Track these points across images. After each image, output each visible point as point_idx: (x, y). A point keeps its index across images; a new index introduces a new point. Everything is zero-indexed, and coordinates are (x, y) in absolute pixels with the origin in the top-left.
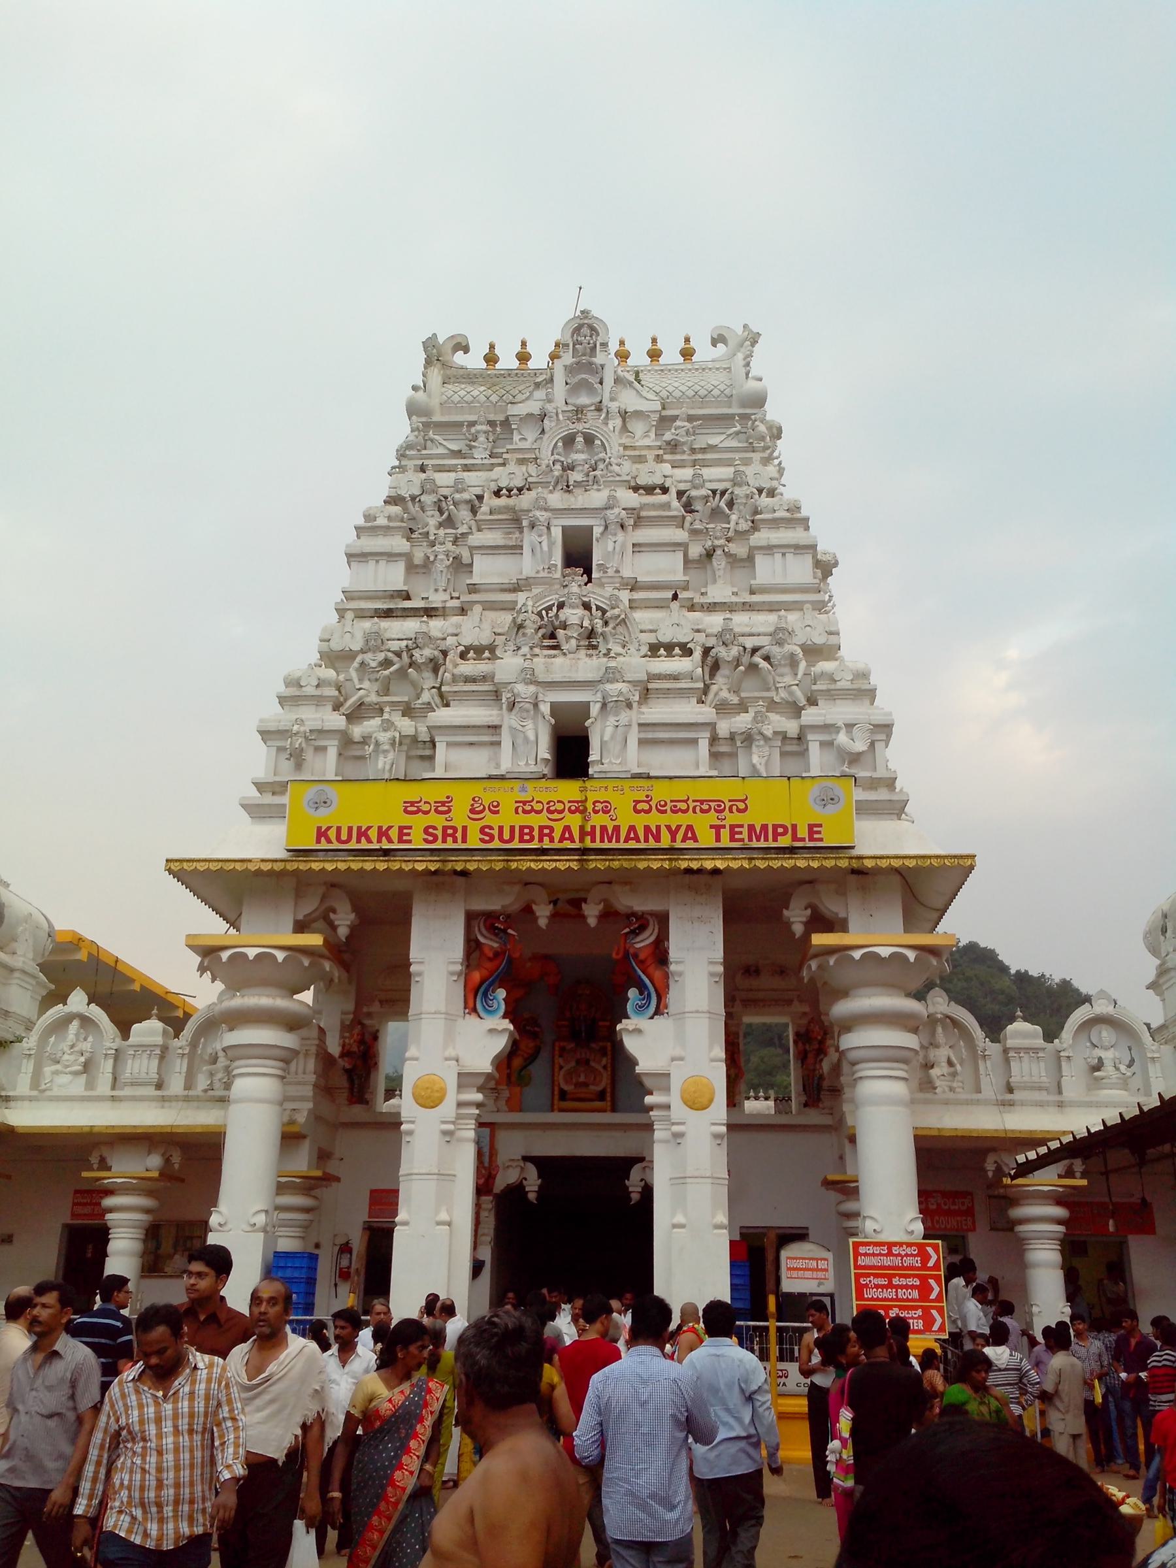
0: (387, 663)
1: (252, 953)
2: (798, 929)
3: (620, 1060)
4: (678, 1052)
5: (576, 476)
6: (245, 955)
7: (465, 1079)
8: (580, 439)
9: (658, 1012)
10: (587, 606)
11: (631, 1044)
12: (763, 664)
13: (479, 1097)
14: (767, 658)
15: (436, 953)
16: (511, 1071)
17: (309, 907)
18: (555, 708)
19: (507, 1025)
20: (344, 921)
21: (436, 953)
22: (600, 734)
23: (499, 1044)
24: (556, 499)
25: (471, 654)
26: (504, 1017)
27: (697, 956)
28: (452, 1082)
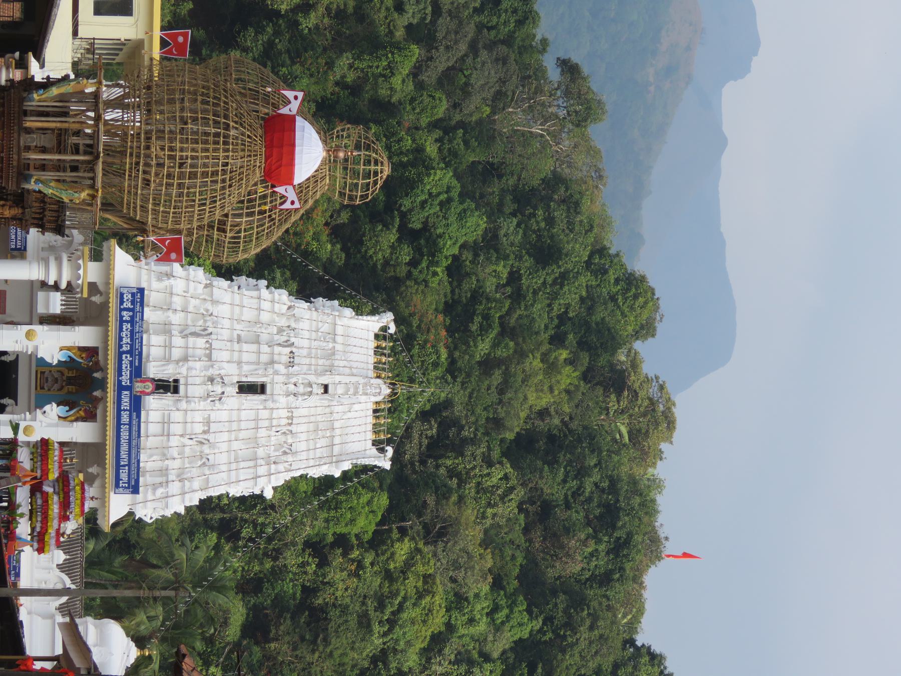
0: (207, 311)
1: (81, 272)
2: (90, 470)
3: (40, 405)
4: (44, 424)
5: (292, 387)
6: (79, 269)
7: (36, 348)
8: (309, 389)
9: (59, 417)
10: (223, 393)
11: (47, 408)
12: (200, 463)
13: (29, 353)
14: (204, 463)
15: (83, 336)
16: (41, 362)
17: (101, 287)
18: (176, 381)
19: (55, 362)
20: (96, 299)
21: (83, 336)
22: (168, 399)
23: (49, 360)
24: (280, 379)
25: (208, 346)
26: (59, 361)
27: (81, 432)
28: (35, 343)
